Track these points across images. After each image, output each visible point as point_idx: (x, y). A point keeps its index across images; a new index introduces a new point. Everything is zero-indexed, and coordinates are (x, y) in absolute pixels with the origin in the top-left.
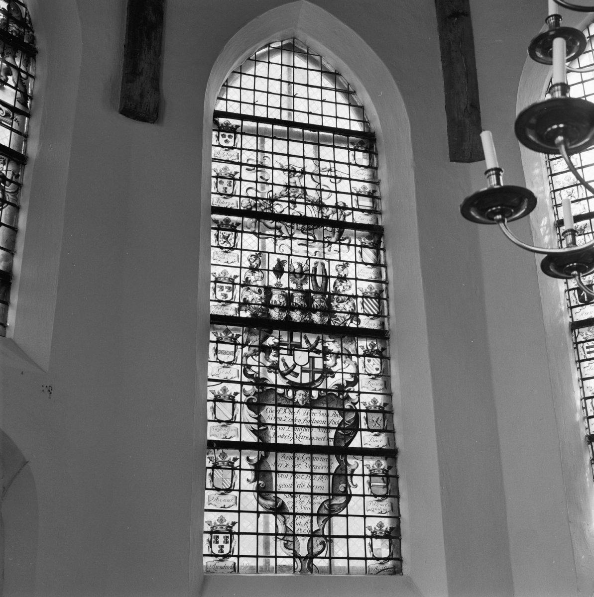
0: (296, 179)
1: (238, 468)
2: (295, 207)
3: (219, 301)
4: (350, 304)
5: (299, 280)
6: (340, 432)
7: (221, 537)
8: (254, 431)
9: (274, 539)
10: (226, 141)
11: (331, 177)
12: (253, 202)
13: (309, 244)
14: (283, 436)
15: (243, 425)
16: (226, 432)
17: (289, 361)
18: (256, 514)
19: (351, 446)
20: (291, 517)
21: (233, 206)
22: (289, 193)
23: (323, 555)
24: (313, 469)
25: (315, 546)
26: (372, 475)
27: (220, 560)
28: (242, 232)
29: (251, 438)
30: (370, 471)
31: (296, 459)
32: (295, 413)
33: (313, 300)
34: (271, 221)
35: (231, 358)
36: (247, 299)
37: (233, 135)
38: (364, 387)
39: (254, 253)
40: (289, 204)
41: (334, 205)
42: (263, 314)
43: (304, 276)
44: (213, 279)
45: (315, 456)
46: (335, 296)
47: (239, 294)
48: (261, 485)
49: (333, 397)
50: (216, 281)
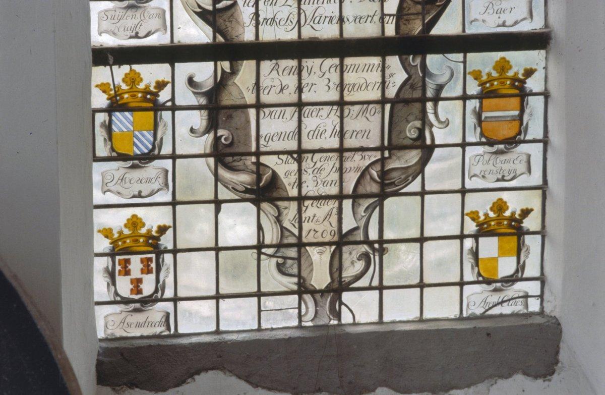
1: (169, 104)
7: (136, 263)
9: (255, 256)
14: (273, 19)
16: (136, 22)
18: (212, 206)
19: (436, 31)
20: (294, 205)
23: (364, 282)
24: (346, 92)
25: (346, 262)
26: (486, 94)
27: (136, 310)
29: (195, 32)
30: (482, 84)
31: (304, 73)
45: (349, 61)
48: (223, 140)
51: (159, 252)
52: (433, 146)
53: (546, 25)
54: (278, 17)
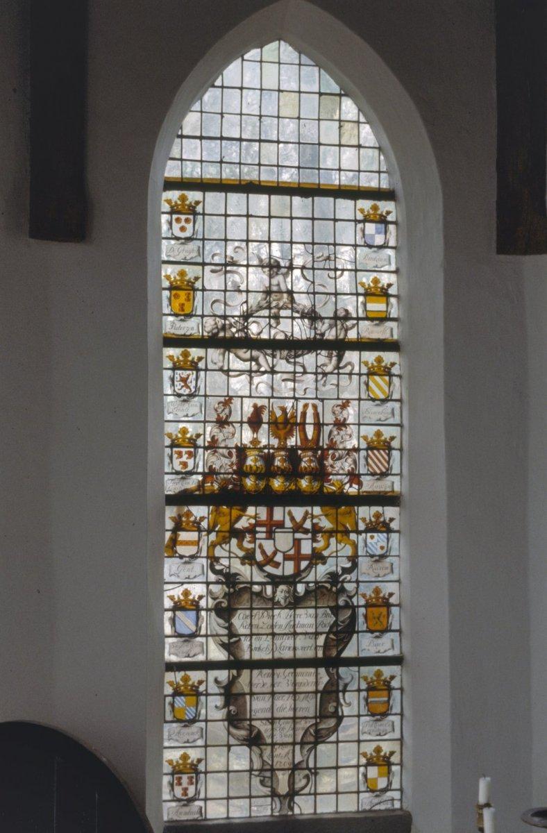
0: (280, 278)
1: (204, 692)
2: (278, 323)
3: (177, 473)
4: (350, 460)
5: (282, 433)
6: (332, 636)
7: (185, 778)
8: (223, 645)
9: (248, 775)
10: (183, 229)
11: (330, 269)
12: (220, 322)
13: (297, 379)
14: (259, 648)
15: (210, 639)
17: (268, 546)
19: (346, 654)
20: (269, 748)
21: (193, 332)
22: (270, 303)
23: (306, 791)
25: (297, 780)
26: (370, 689)
27: (184, 805)
28: (206, 370)
29: (217, 654)
30: (368, 683)
31: (275, 677)
32: (275, 618)
33: (300, 459)
34: (245, 350)
35: (191, 550)
36: (214, 466)
37: (191, 217)
38: (365, 573)
39: (222, 399)
40: (270, 320)
41: (332, 315)
42: (235, 485)
43: (289, 426)
44: (168, 442)
45: (298, 670)
46: (331, 452)
47: (202, 461)
48: (232, 713)
49: (325, 590)
50: (172, 446)
51: (197, 772)
52: (343, 716)
53: (401, 653)
54: (262, 647)
